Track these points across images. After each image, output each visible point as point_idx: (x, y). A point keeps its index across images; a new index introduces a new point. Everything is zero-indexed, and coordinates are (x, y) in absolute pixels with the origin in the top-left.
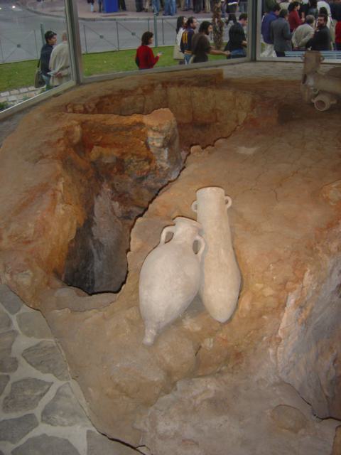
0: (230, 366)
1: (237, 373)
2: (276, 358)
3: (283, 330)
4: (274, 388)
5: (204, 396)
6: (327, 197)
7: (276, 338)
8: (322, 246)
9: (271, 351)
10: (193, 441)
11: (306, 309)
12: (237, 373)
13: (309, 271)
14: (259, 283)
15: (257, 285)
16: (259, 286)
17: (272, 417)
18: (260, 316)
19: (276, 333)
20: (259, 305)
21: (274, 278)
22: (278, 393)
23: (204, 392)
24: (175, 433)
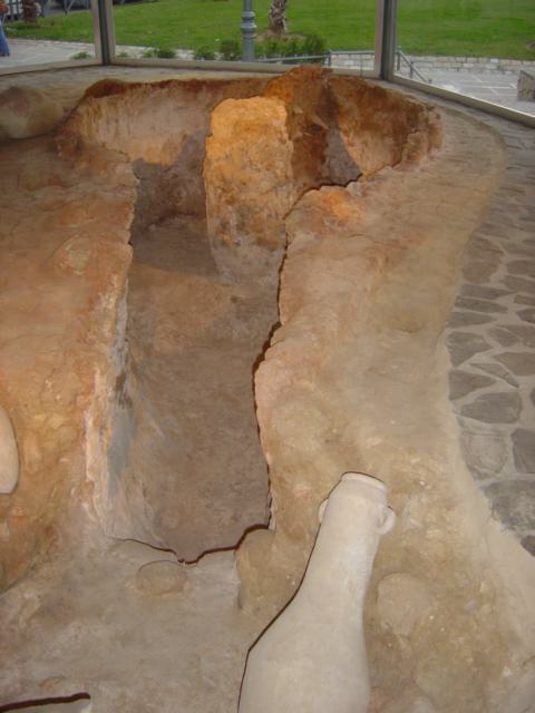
0: (43, 552)
1: (57, 557)
2: (96, 513)
3: (92, 469)
4: (115, 553)
5: (27, 614)
6: (69, 267)
7: (86, 484)
8: (94, 333)
9: (86, 506)
10: (54, 678)
11: (106, 429)
12: (57, 557)
13: (99, 372)
14: (38, 414)
15: (36, 417)
16: (40, 418)
17: (141, 587)
18: (57, 460)
19: (85, 478)
20: (51, 446)
21: (58, 397)
22: (122, 556)
23: (23, 607)
24: (22, 683)
